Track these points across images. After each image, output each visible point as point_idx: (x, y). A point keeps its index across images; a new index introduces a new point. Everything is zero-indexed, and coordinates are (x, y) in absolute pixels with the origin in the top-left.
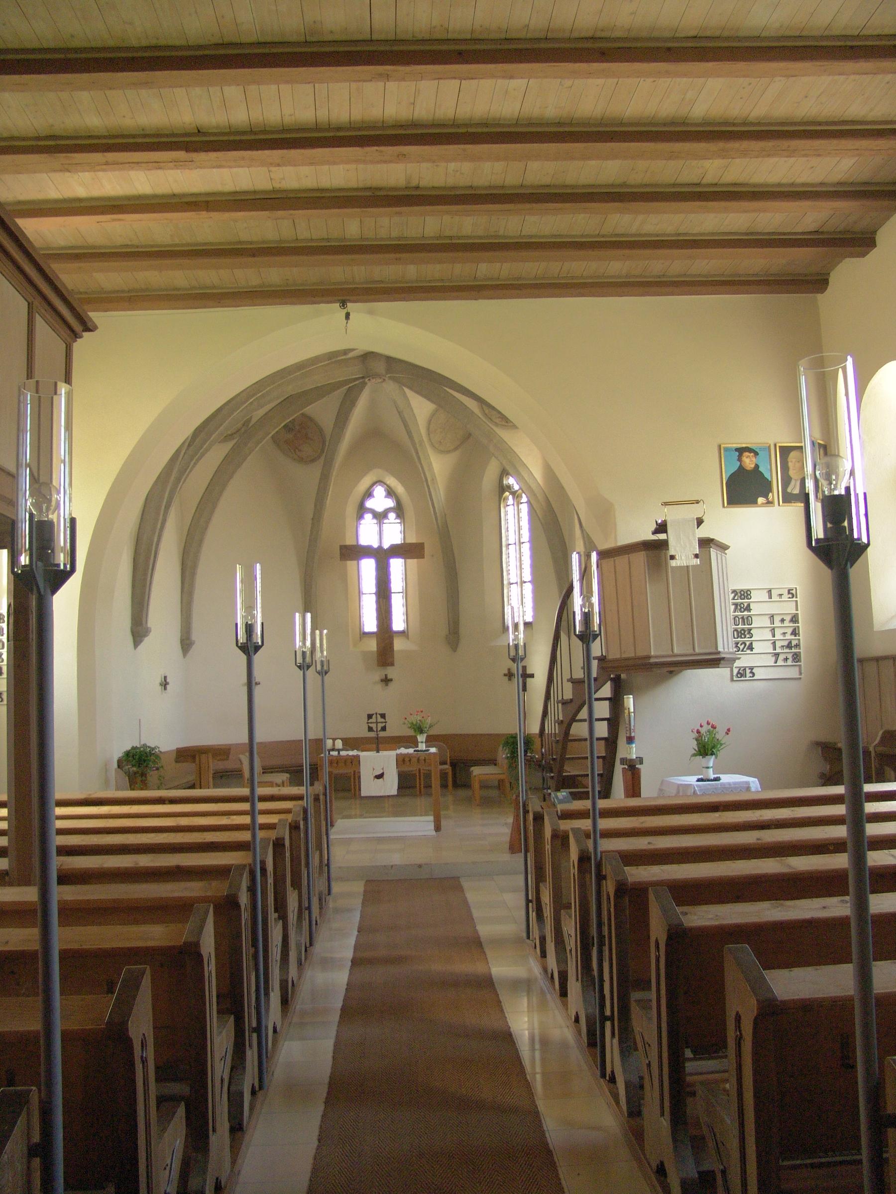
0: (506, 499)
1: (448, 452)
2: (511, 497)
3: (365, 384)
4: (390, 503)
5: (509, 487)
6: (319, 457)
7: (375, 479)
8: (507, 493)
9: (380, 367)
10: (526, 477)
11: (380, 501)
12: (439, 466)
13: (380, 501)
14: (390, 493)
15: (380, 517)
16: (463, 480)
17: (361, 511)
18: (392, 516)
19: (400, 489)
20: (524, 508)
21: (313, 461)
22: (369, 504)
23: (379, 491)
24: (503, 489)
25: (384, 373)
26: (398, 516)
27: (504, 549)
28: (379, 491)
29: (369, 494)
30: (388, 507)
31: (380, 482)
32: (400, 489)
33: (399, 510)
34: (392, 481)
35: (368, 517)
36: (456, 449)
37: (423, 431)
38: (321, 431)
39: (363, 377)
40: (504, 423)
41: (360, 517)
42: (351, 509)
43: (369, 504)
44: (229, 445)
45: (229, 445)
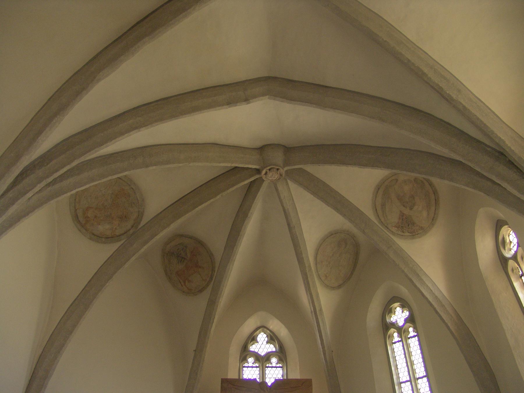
0: (392, 336)
1: (333, 288)
2: (396, 335)
3: (261, 181)
4: (271, 348)
5: (394, 325)
6: (208, 285)
7: (259, 324)
8: (392, 330)
9: (278, 157)
10: (430, 285)
11: (262, 345)
12: (327, 300)
13: (262, 345)
14: (272, 338)
15: (263, 361)
16: (348, 314)
17: (245, 353)
18: (274, 360)
19: (283, 332)
20: (414, 343)
21: (201, 291)
22: (253, 348)
23: (262, 337)
24: (387, 327)
25: (282, 165)
26: (280, 360)
27: (396, 387)
28: (262, 337)
29: (253, 339)
30: (270, 350)
31: (263, 328)
32: (283, 332)
33: (282, 354)
34: (276, 325)
35: (251, 360)
36: (339, 287)
37: (311, 259)
38: (211, 255)
39: (258, 171)
40: (400, 233)
41: (244, 359)
42: (234, 350)
43: (253, 348)
44: (115, 246)
45: (115, 246)
